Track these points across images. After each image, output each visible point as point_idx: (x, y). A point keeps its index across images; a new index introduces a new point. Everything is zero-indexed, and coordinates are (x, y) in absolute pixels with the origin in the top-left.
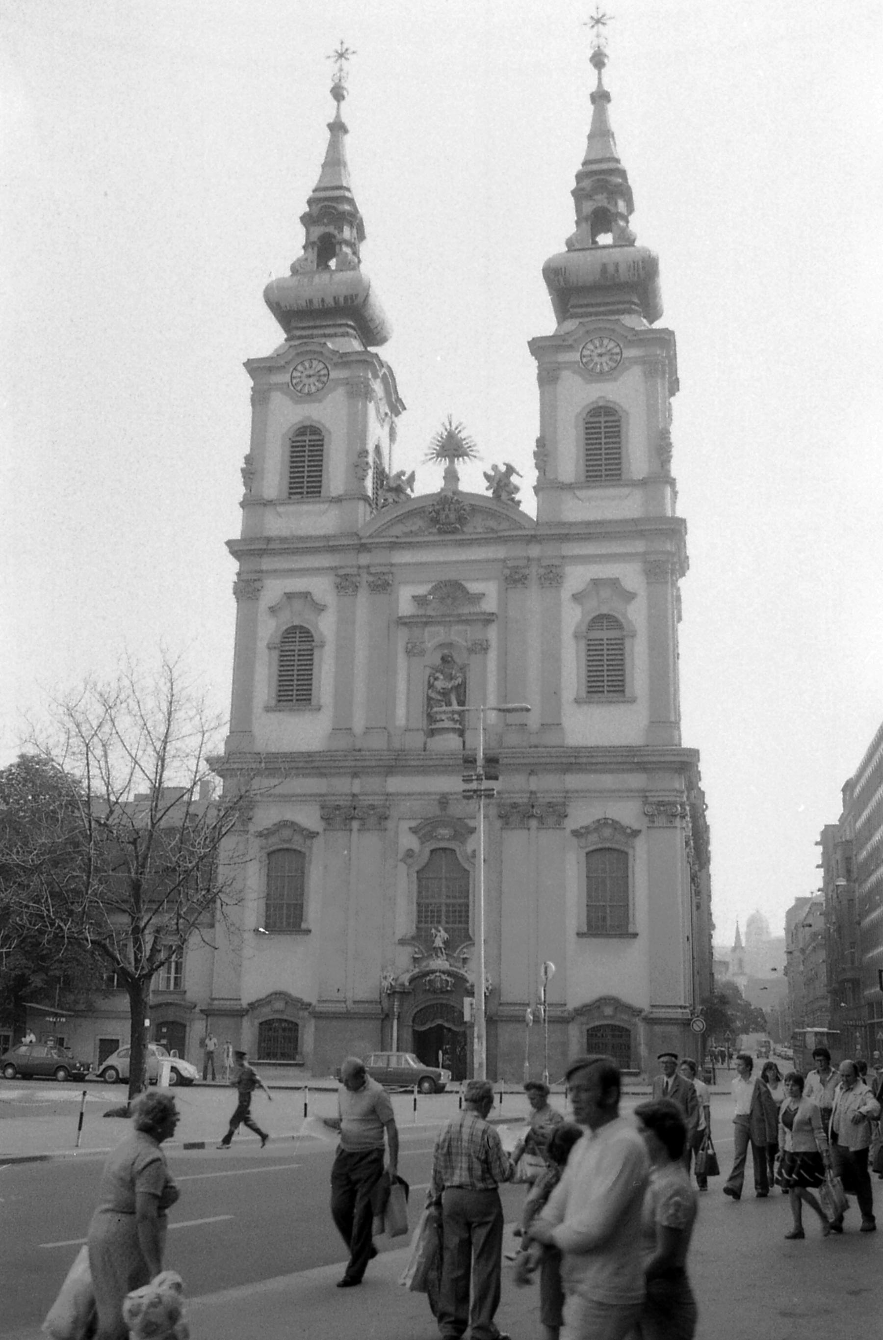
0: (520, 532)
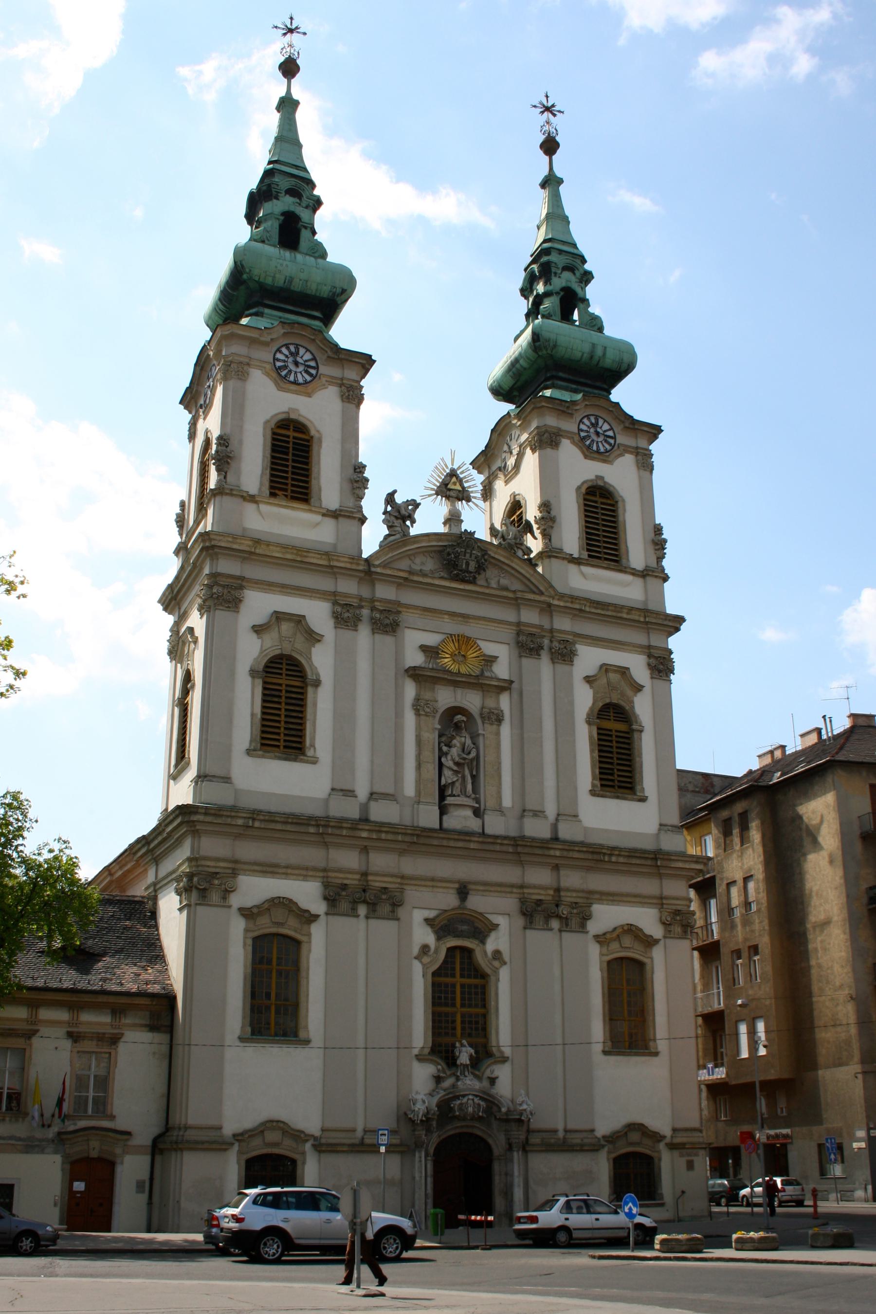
0: (537, 598)
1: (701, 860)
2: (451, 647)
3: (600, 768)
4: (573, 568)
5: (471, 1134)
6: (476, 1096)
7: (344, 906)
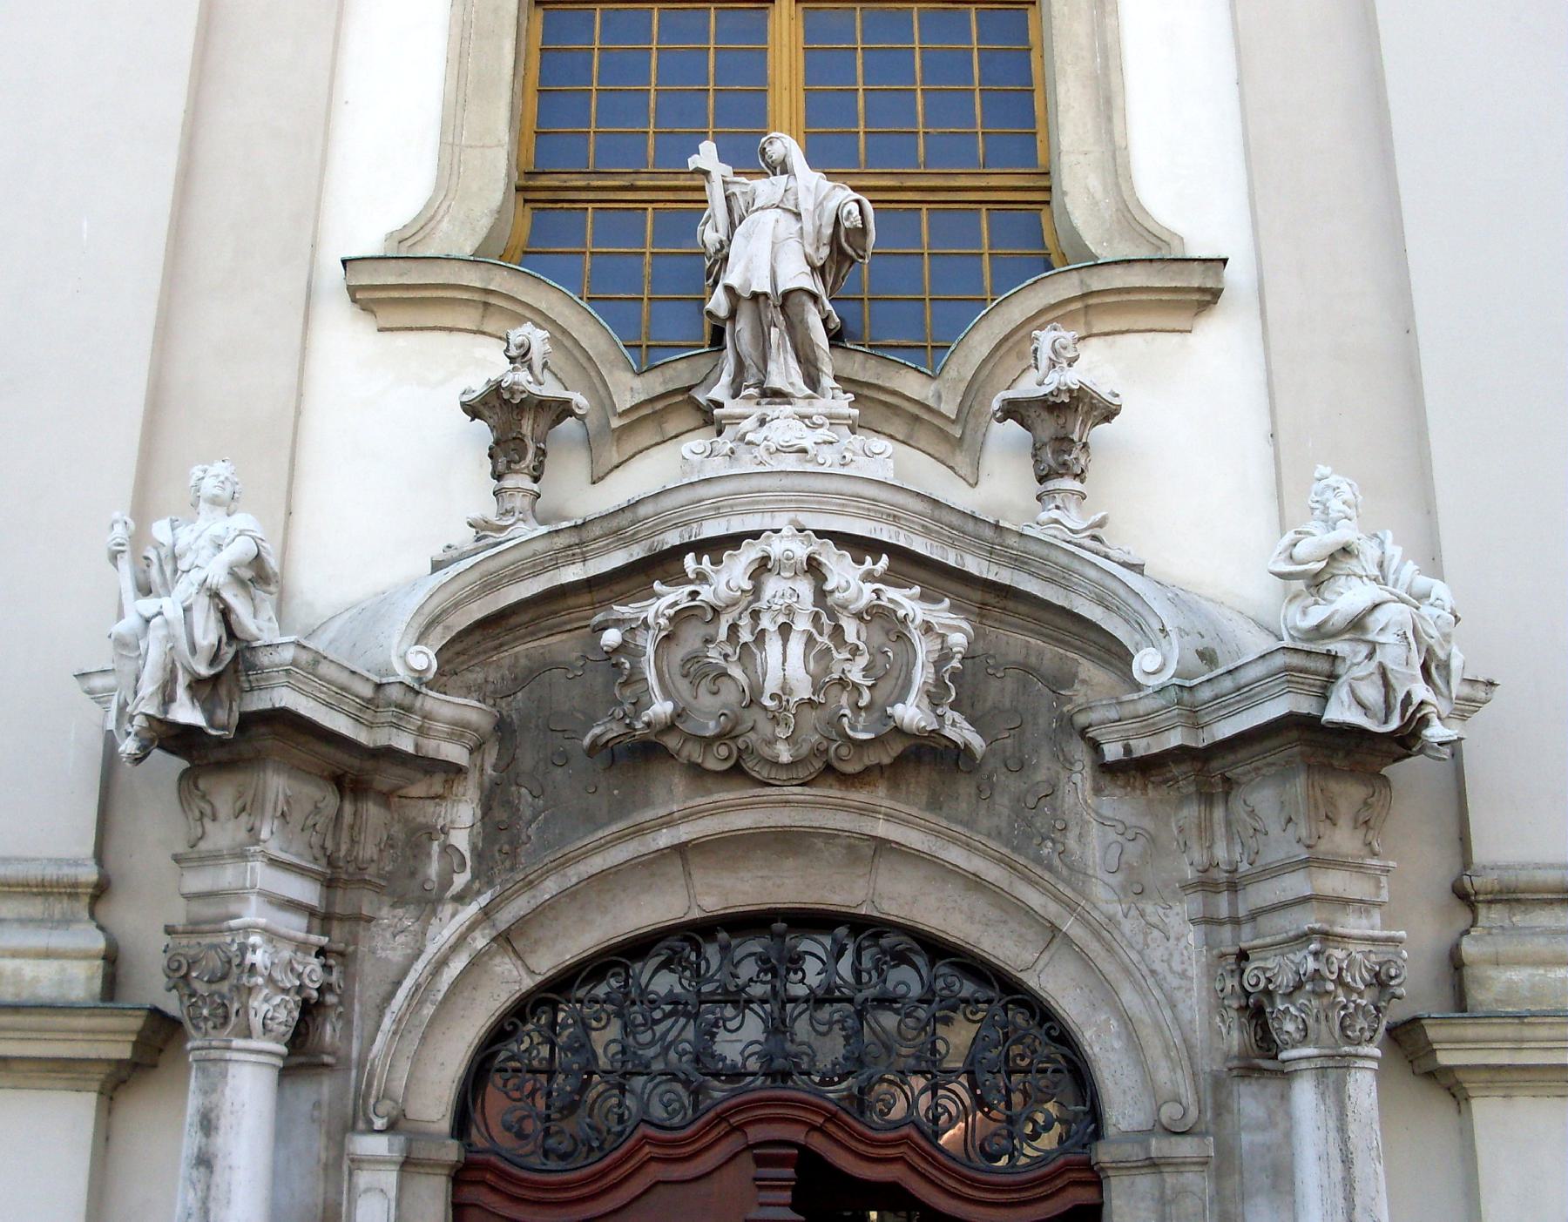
6: (860, 546)
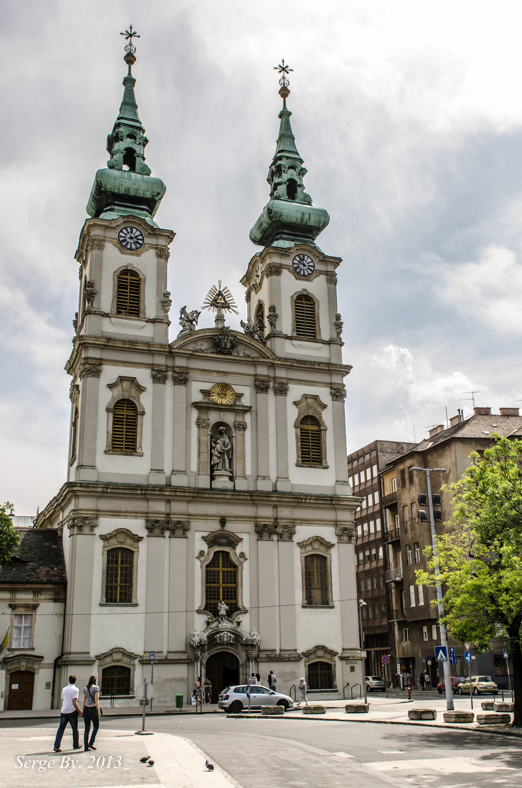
0: (266, 360)
1: (358, 500)
2: (218, 390)
3: (302, 451)
4: (288, 342)
5: (227, 653)
6: (229, 632)
7: (157, 531)
